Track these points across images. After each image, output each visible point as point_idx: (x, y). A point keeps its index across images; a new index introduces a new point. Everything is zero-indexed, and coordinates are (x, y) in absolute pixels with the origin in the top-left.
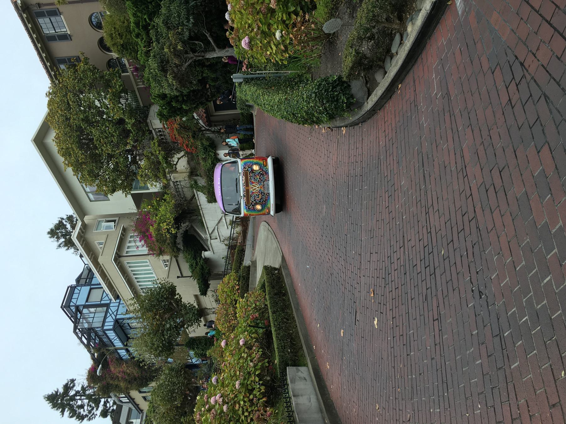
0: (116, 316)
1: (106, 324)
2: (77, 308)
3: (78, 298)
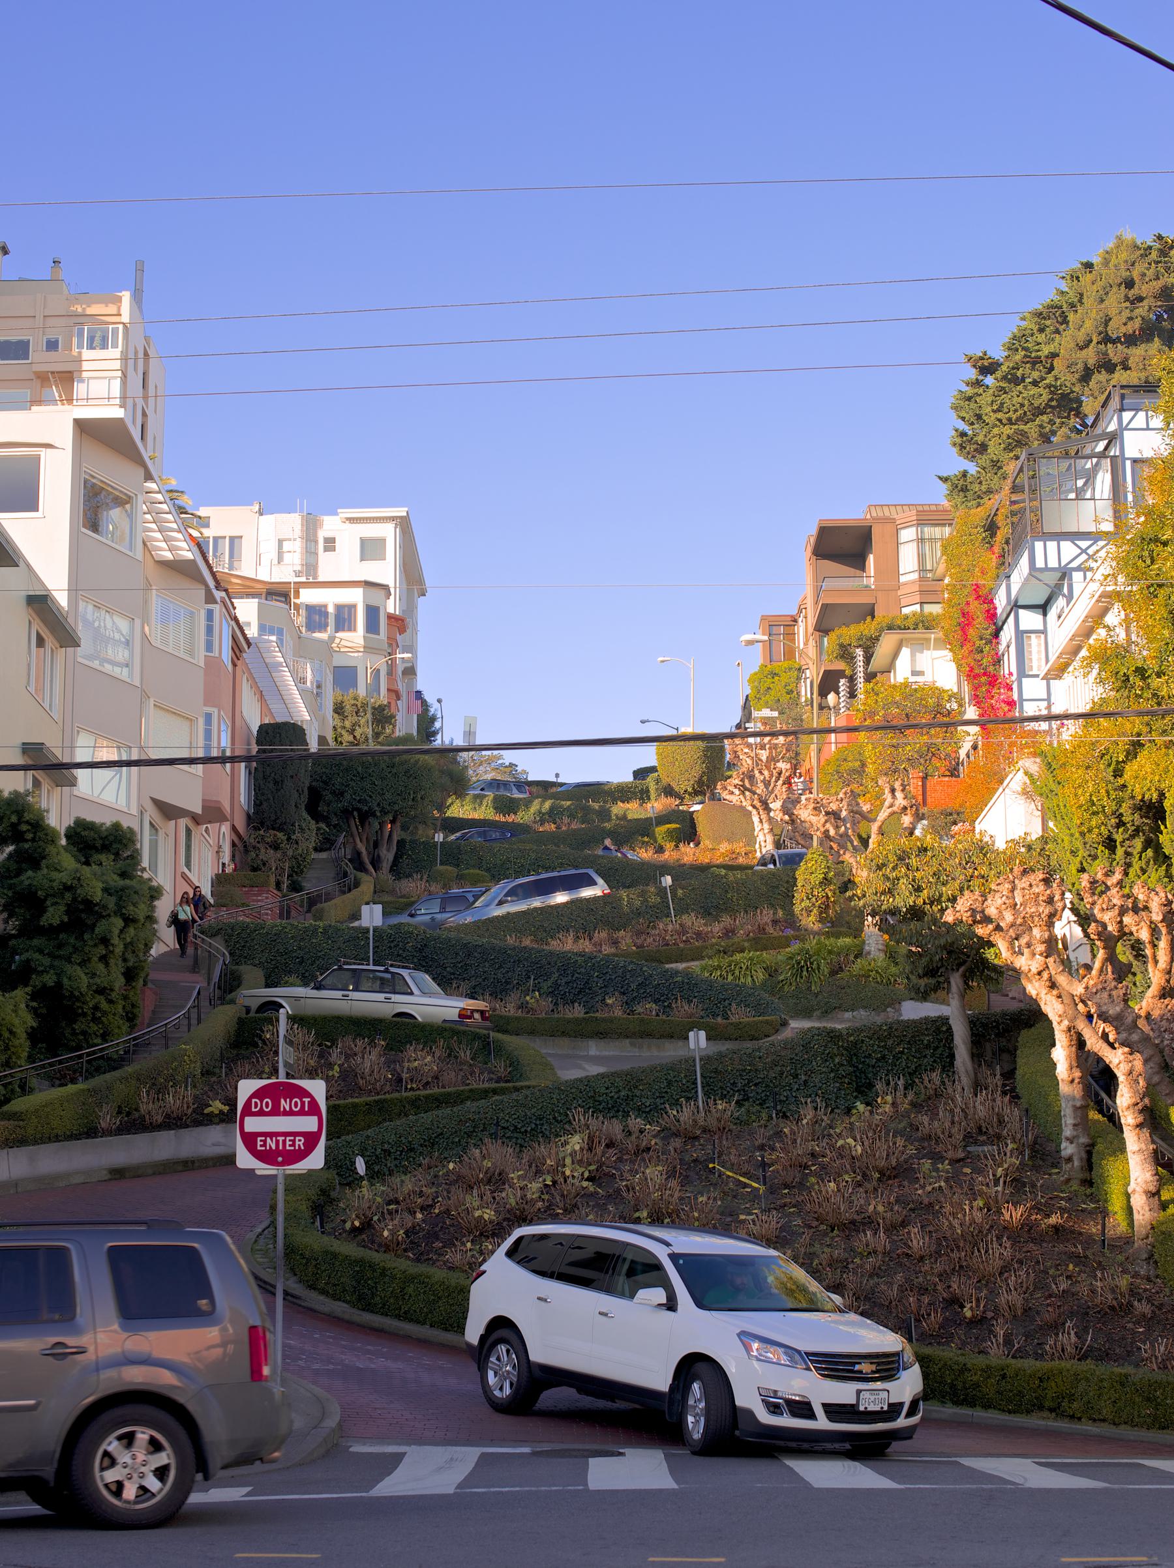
0: (1078, 569)
1: (1052, 545)
2: (1113, 438)
3: (1148, 429)
